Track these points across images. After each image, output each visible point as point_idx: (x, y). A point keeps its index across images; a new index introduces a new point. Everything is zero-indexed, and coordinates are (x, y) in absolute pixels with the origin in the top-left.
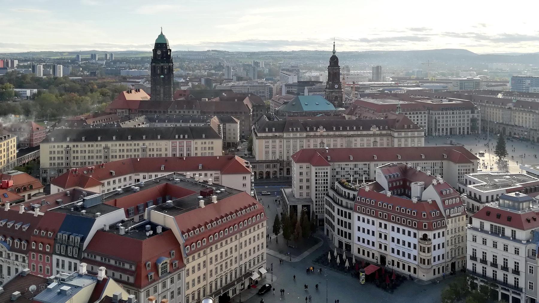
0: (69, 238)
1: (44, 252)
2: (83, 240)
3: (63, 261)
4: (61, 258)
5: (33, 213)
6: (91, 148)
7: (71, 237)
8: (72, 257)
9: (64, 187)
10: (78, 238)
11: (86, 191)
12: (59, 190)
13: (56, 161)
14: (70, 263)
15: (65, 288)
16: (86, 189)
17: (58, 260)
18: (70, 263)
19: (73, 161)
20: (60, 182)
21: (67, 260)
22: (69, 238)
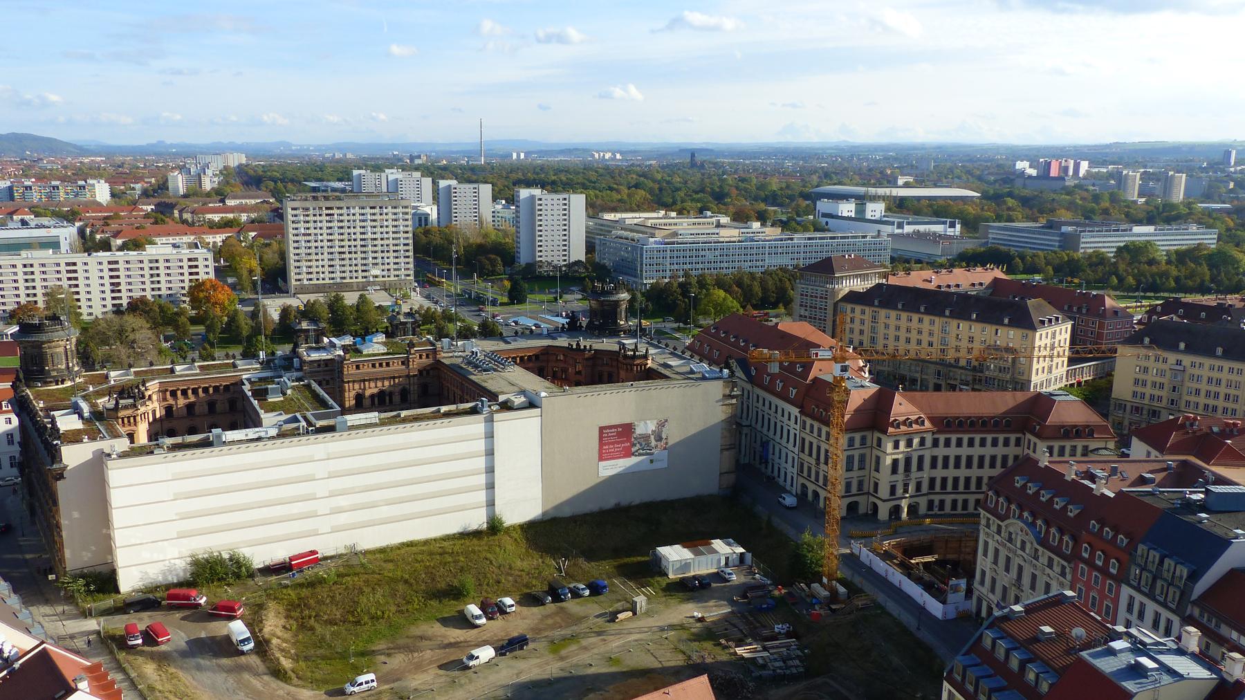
0: (1161, 562)
1: (1104, 571)
2: (1194, 577)
3: (1142, 605)
4: (1139, 598)
5: (1093, 486)
6: (1234, 377)
7: (1167, 561)
8: (1164, 605)
9: (1161, 449)
10: (1183, 571)
11: (1214, 473)
12: (1149, 454)
13: (1148, 391)
14: (1157, 615)
15: (1144, 661)
16: (1214, 469)
17: (1131, 598)
18: (1157, 615)
19: (1186, 398)
20: (1156, 436)
21: (1151, 607)
22: (1161, 562)
